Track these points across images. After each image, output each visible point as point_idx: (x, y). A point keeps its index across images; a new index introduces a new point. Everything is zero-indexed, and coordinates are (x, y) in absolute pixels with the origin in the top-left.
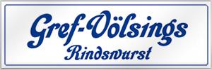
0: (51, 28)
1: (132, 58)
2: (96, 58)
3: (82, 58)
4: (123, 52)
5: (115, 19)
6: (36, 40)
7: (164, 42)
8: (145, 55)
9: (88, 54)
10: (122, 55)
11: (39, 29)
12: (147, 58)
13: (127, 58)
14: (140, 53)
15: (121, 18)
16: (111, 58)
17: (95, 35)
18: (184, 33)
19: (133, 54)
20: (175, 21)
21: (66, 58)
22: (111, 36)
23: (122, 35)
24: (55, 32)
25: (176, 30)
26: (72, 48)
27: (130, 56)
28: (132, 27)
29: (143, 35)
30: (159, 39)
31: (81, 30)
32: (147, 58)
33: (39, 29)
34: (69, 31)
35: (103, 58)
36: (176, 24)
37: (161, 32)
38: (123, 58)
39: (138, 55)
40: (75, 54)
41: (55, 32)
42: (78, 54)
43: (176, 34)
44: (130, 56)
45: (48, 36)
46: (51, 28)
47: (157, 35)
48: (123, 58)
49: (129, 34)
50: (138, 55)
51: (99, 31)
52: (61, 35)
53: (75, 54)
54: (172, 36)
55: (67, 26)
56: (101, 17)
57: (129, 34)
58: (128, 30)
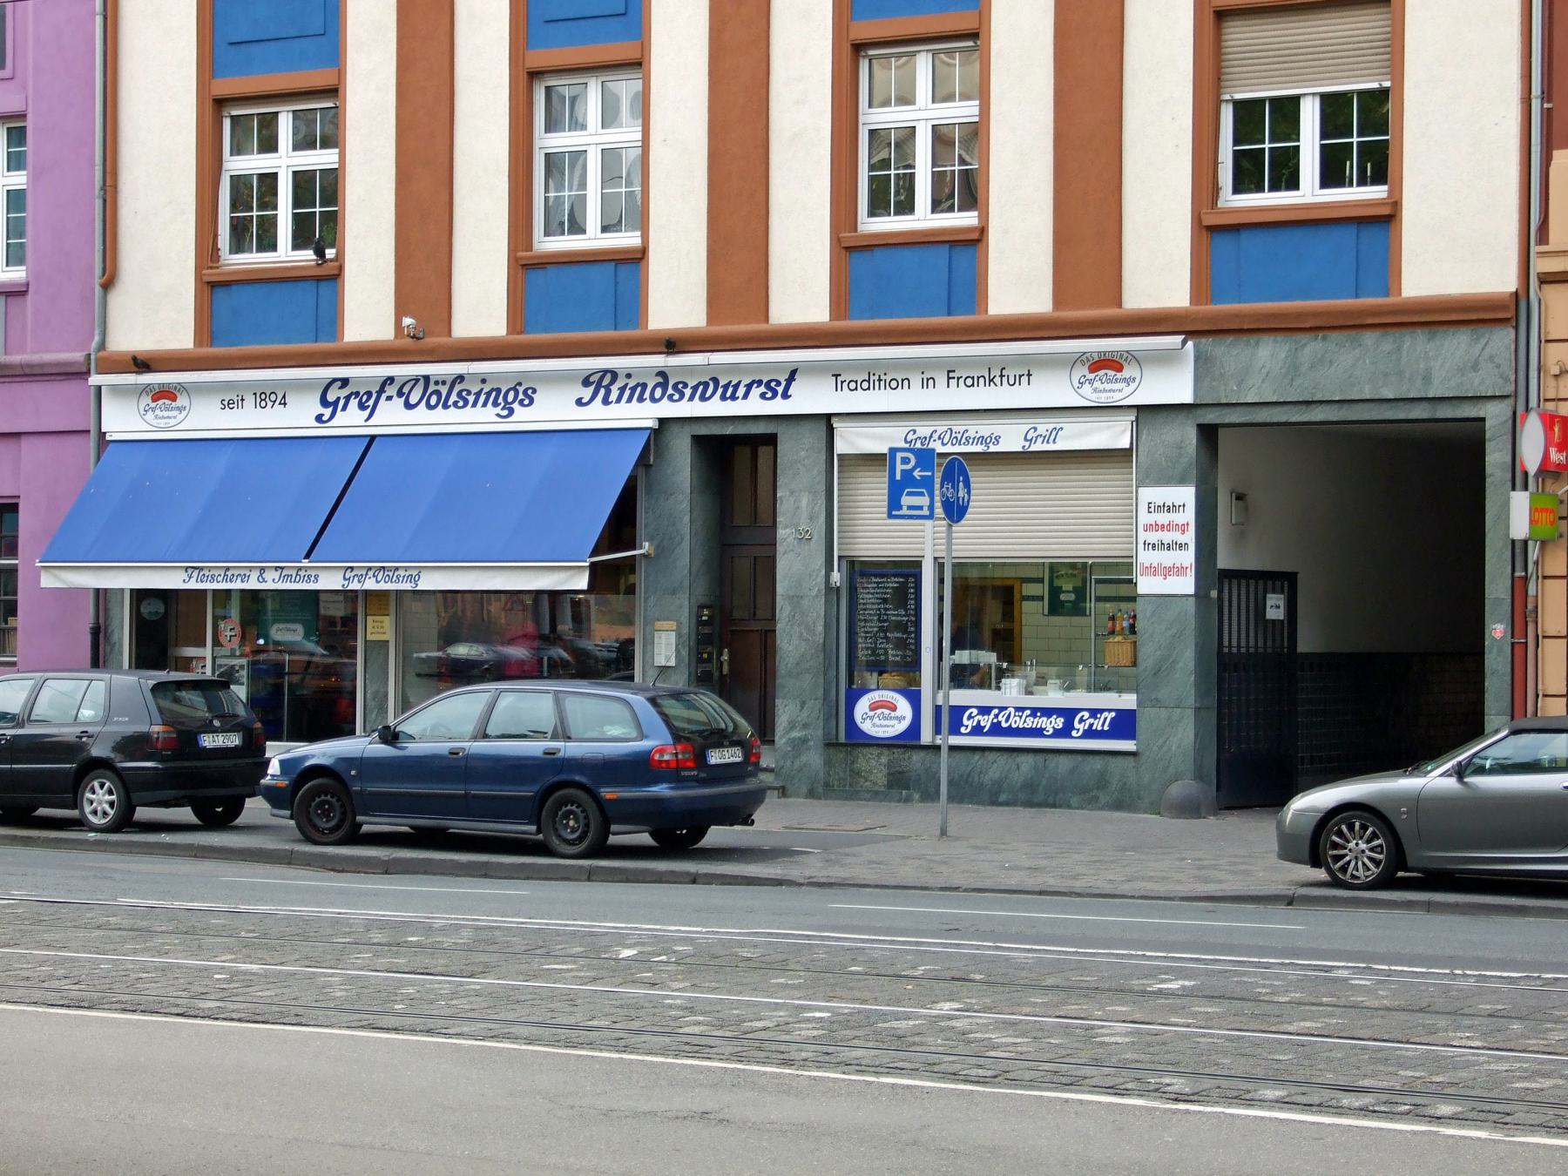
0: (348, 398)
1: (746, 396)
2: (653, 400)
3: (619, 400)
4: (722, 383)
5: (437, 383)
6: (327, 412)
7: (505, 412)
8: (780, 389)
9: (633, 390)
10: (720, 391)
11: (331, 397)
12: (785, 396)
13: (733, 397)
14: (768, 385)
15: (444, 383)
16: (691, 398)
17: (408, 406)
18: (532, 401)
19: (749, 387)
20: (520, 384)
21: (579, 402)
22: (430, 407)
23: (446, 406)
24: (354, 402)
25: (521, 396)
26: (595, 378)
27: (741, 391)
28: (459, 394)
29: (474, 405)
30: (498, 410)
31: (389, 398)
32: (785, 396)
33: (331, 397)
34: (371, 403)
35: (671, 398)
36: (521, 390)
37: (500, 400)
38: (723, 398)
39: (762, 389)
40: (602, 391)
41: (354, 402)
42: (608, 392)
43: (521, 403)
44: (741, 391)
45: (344, 409)
46: (348, 398)
47: (495, 404)
48: (723, 398)
49: (455, 404)
50: (762, 389)
51: (413, 400)
52: (362, 406)
53: (602, 391)
54: (516, 406)
55: (369, 394)
56: (417, 381)
57: (455, 404)
58: (454, 398)
